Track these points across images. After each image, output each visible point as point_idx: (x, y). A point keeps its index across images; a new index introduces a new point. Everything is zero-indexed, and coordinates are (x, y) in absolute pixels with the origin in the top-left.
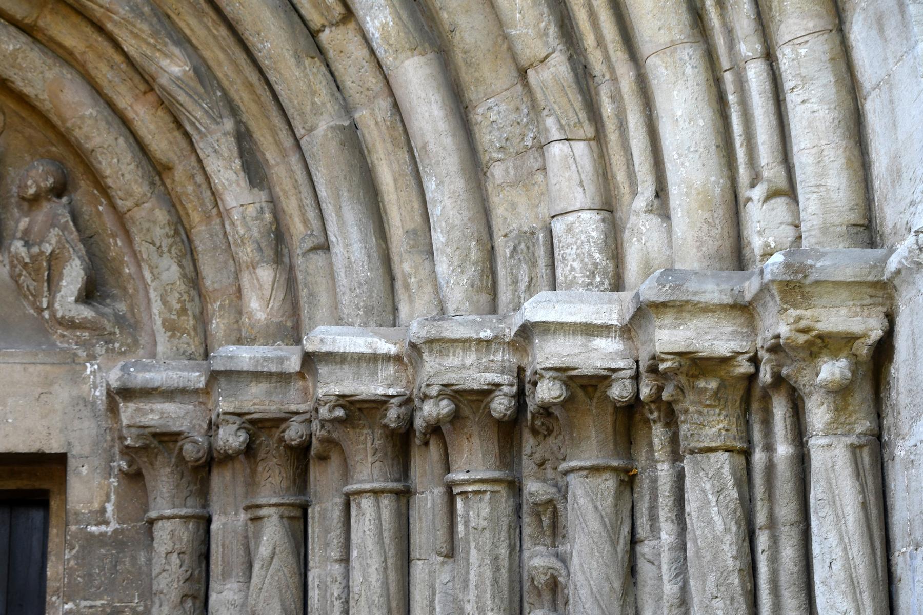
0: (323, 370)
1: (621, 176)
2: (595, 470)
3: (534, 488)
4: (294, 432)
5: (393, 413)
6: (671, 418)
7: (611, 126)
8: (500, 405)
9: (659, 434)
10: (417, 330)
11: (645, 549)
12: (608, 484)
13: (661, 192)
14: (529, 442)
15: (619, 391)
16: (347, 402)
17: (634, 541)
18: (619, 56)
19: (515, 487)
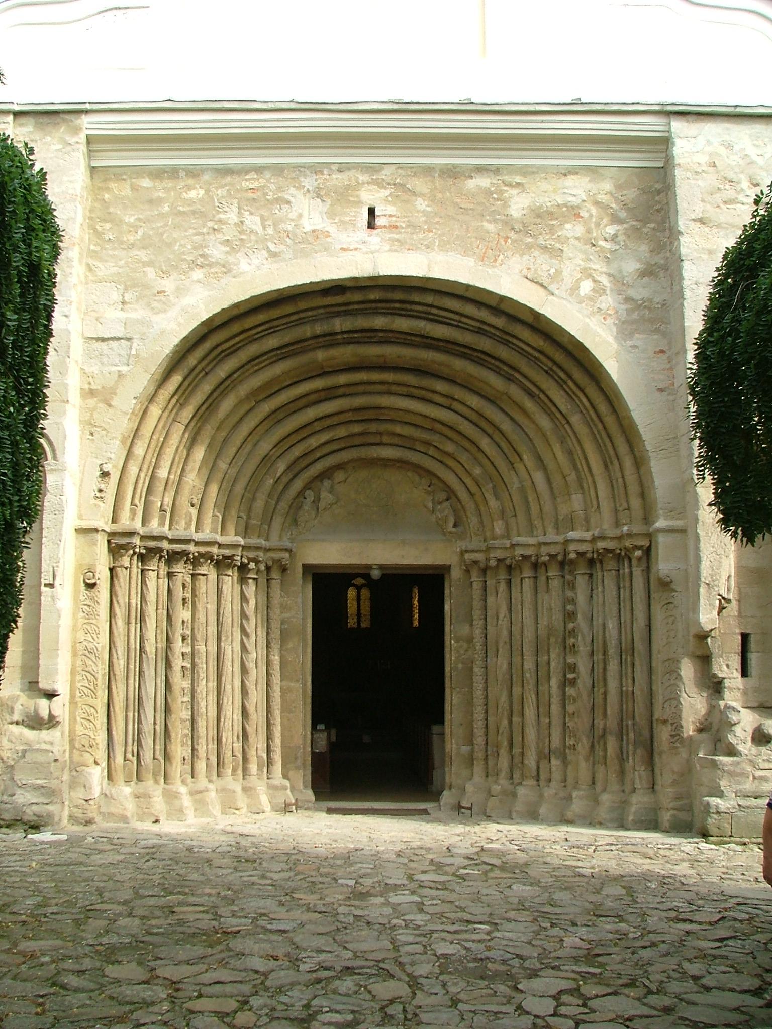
0: (516, 548)
1: (589, 502)
2: (583, 574)
3: (568, 577)
4: (508, 562)
5: (533, 558)
6: (601, 562)
7: (586, 490)
8: (560, 558)
9: (598, 565)
10: (542, 539)
11: (594, 592)
12: (586, 577)
13: (598, 507)
14: (567, 567)
15: (589, 555)
16: (522, 556)
17: (592, 590)
18: (588, 475)
19: (563, 577)
